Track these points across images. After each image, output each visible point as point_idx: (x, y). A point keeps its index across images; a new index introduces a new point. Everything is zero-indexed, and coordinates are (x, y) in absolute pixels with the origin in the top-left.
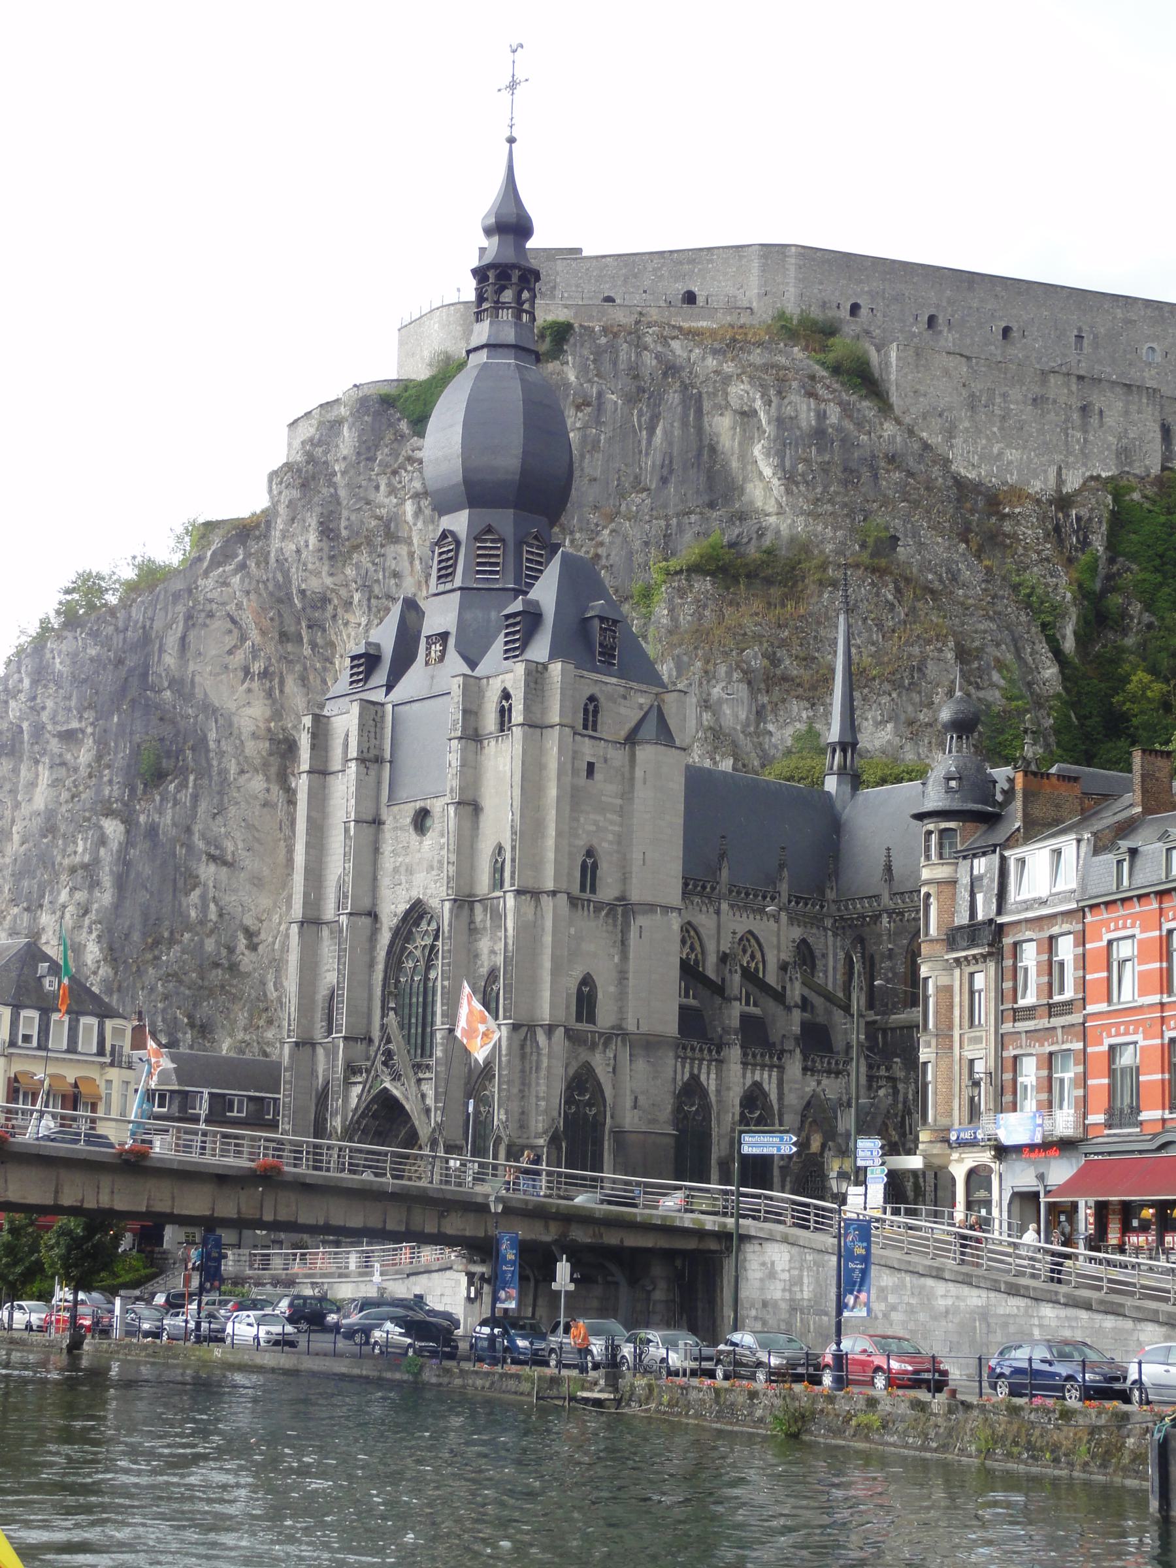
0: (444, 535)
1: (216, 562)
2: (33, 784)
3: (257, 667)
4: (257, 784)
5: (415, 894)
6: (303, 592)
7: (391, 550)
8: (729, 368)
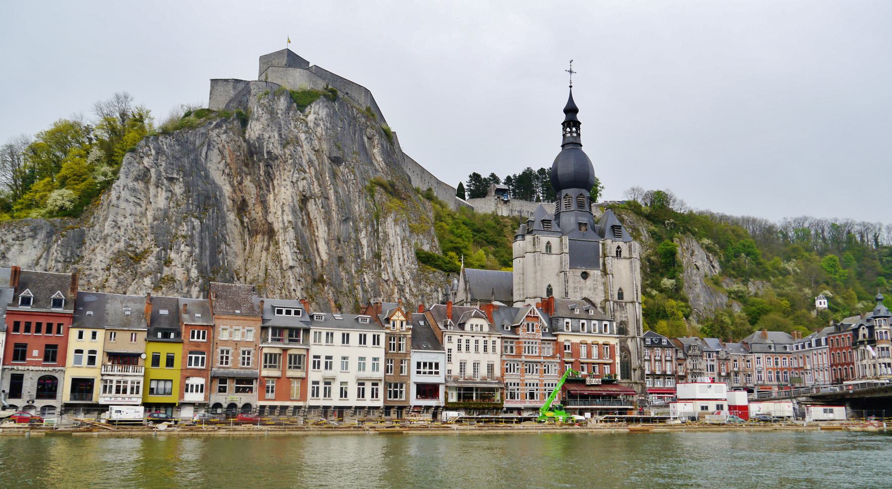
1: (218, 126)
2: (156, 196)
3: (227, 171)
4: (232, 216)
6: (269, 153)
7: (299, 148)
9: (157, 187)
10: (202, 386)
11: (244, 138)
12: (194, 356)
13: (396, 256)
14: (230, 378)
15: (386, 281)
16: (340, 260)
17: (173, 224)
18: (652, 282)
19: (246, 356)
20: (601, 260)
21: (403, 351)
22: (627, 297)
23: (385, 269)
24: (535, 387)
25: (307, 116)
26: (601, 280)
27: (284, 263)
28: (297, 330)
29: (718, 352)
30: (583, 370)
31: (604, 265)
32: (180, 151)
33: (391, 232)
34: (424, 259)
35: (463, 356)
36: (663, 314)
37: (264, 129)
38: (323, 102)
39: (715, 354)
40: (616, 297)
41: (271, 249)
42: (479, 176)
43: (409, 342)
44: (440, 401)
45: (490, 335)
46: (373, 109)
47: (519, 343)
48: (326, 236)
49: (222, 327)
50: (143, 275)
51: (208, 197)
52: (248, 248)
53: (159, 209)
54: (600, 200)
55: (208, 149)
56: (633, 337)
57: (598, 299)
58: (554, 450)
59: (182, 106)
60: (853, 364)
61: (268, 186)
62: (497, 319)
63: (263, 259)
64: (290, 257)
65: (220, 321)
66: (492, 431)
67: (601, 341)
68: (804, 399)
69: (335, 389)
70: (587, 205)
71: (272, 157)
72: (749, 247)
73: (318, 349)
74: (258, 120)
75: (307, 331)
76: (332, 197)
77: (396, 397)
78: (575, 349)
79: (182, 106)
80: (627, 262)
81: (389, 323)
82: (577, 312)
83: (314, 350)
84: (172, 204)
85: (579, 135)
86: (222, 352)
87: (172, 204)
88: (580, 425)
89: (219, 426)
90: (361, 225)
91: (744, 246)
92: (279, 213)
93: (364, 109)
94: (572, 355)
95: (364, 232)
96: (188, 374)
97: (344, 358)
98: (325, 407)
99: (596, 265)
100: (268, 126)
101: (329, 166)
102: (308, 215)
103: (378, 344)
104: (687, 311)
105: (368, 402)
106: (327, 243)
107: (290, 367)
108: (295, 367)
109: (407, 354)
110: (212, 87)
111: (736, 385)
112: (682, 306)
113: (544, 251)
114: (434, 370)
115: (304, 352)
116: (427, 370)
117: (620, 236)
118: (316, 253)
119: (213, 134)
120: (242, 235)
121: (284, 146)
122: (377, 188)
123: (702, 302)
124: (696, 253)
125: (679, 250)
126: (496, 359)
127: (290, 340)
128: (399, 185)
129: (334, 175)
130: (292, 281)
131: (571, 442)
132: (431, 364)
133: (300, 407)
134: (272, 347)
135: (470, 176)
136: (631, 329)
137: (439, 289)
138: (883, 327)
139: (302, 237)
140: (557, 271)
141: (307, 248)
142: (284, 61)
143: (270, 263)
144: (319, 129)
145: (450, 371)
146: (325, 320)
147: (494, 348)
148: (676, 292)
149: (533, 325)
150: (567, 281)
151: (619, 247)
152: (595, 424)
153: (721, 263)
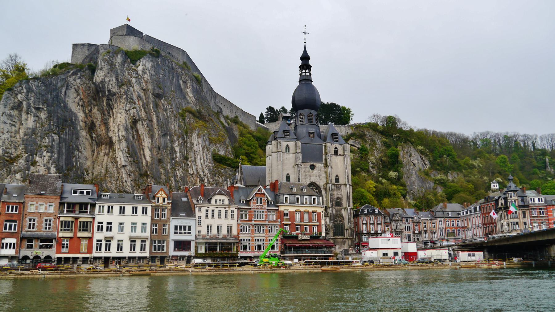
0: (310, 113)
1: (74, 74)
2: (27, 120)
3: (81, 103)
4: (84, 133)
5: (312, 181)
7: (131, 88)
8: (183, 72)
9: (28, 114)
10: (14, 244)
11: (92, 81)
12: (8, 223)
13: (199, 158)
14: (35, 238)
15: (192, 175)
16: (160, 161)
17: (39, 138)
18: (383, 174)
19: (48, 223)
20: (324, 157)
21: (165, 218)
22: (341, 181)
23: (191, 167)
24: (262, 242)
25: (137, 67)
26: (323, 170)
27: (119, 163)
28: (86, 205)
29: (413, 218)
30: (297, 230)
31: (326, 160)
32: (44, 90)
33: (195, 142)
34: (218, 160)
35: (210, 221)
36: (387, 194)
37: (105, 76)
38: (149, 58)
39: (411, 219)
40: (334, 181)
41: (111, 154)
42: (273, 109)
43: (169, 212)
44: (192, 252)
45: (229, 206)
46: (188, 63)
47: (251, 212)
48: (150, 146)
49: (30, 203)
50: (15, 172)
51: (66, 121)
52: (95, 154)
53: (28, 128)
54: (351, 122)
55: (67, 89)
56: (346, 208)
57: (321, 183)
58: (276, 285)
59: (53, 61)
60: (496, 223)
61: (109, 113)
62: (236, 196)
63: (105, 161)
64: (123, 159)
65: (28, 199)
66: (218, 273)
67: (311, 210)
68: (456, 247)
69: (114, 245)
70: (314, 120)
71: (111, 94)
72: (449, 151)
73: (101, 217)
74: (101, 69)
75: (93, 205)
76: (155, 120)
77: (159, 250)
78: (292, 215)
79: (53, 61)
80: (342, 158)
81: (155, 199)
82: (294, 190)
83: (99, 218)
84: (38, 125)
85: (311, 74)
86: (30, 220)
87: (38, 125)
88: (286, 267)
89: (10, 271)
90: (175, 138)
91: (446, 150)
92: (116, 130)
93: (181, 63)
94: (289, 220)
95: (177, 143)
96: (3, 236)
97: (121, 224)
98: (105, 257)
99: (320, 160)
100: (108, 73)
101: (154, 100)
102: (137, 131)
103: (146, 213)
104: (404, 192)
105: (138, 253)
106: (151, 150)
107: (80, 230)
108: (83, 230)
109: (168, 220)
110: (74, 49)
111: (425, 239)
112: (401, 189)
113: (284, 151)
114: (187, 231)
115: (91, 220)
116: (183, 231)
117: (337, 141)
118: (143, 157)
119: (71, 79)
120: (91, 146)
121: (120, 87)
122: (187, 114)
123: (416, 187)
124: (413, 155)
125: (401, 153)
126: (234, 223)
127: (80, 212)
128: (204, 112)
129: (156, 106)
130: (124, 175)
131: (287, 281)
132: (185, 227)
133: (88, 258)
134: (67, 217)
135: (267, 109)
136: (345, 203)
137: (228, 180)
138: (513, 198)
139: (133, 146)
140: (293, 164)
141: (136, 153)
142: (125, 31)
143: (109, 163)
144: (146, 76)
145: (199, 232)
146: (110, 197)
147: (232, 216)
148: (398, 181)
149: (261, 199)
150: (299, 171)
151: (336, 148)
152: (297, 265)
153: (430, 162)
